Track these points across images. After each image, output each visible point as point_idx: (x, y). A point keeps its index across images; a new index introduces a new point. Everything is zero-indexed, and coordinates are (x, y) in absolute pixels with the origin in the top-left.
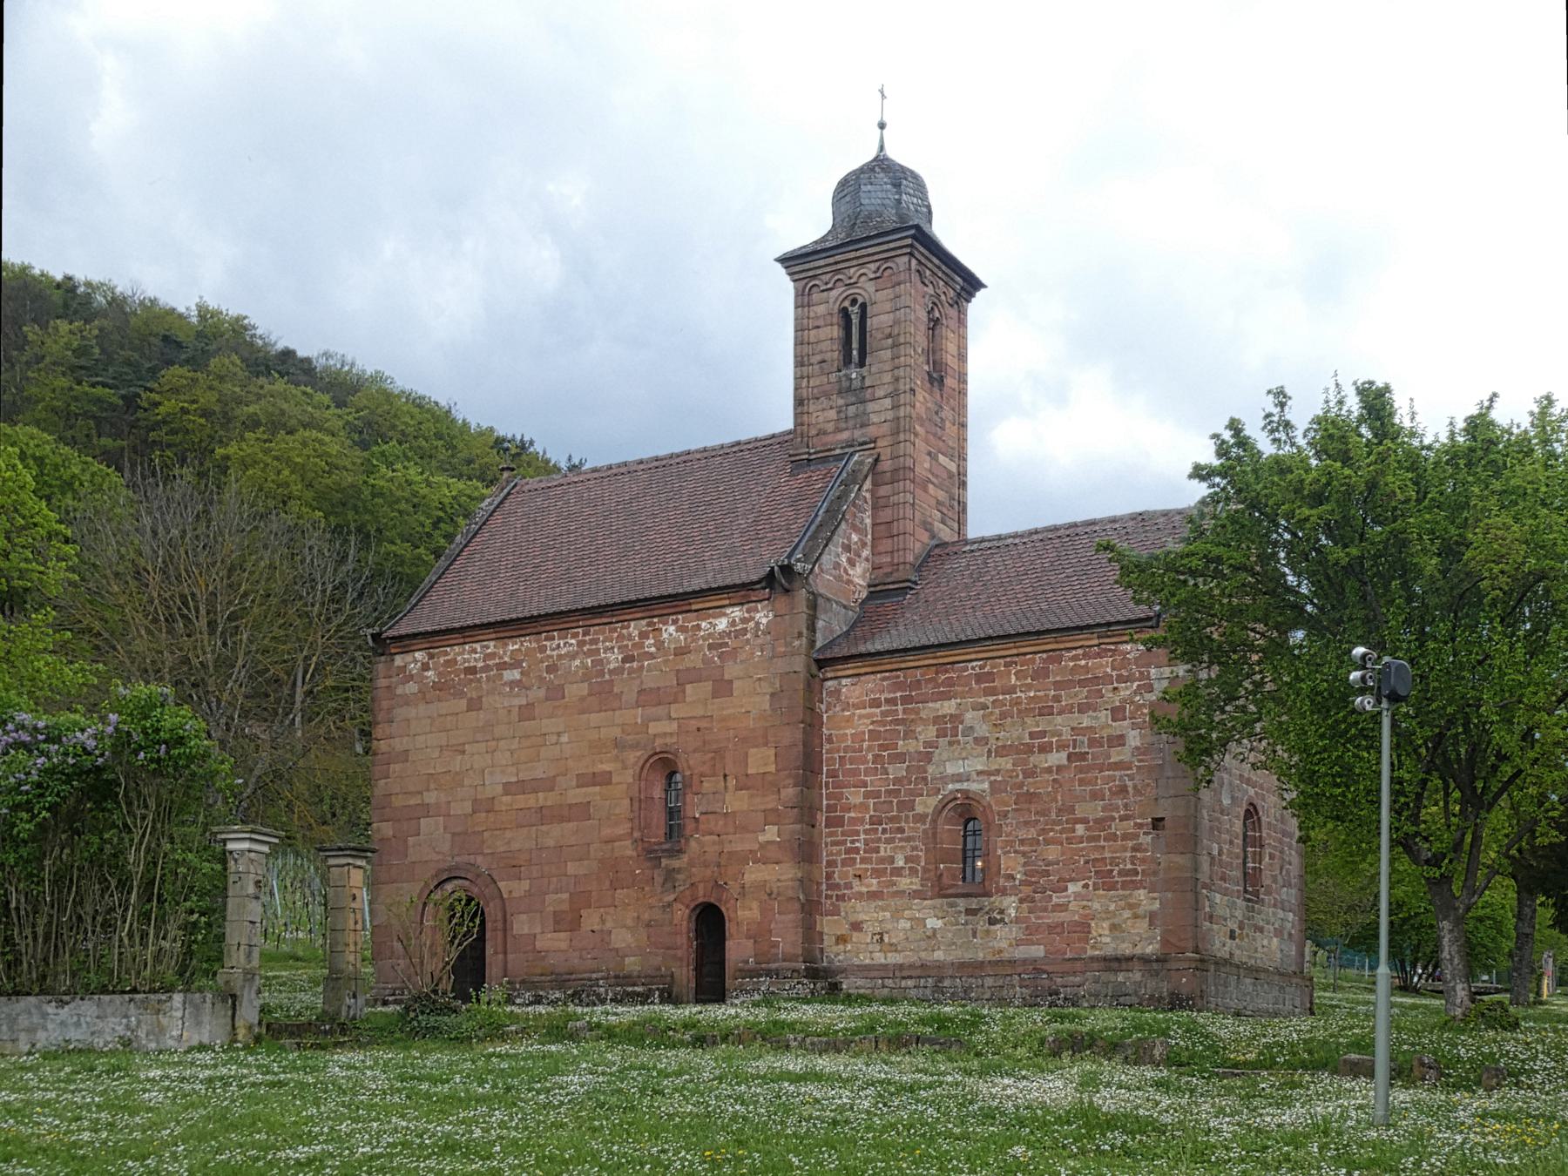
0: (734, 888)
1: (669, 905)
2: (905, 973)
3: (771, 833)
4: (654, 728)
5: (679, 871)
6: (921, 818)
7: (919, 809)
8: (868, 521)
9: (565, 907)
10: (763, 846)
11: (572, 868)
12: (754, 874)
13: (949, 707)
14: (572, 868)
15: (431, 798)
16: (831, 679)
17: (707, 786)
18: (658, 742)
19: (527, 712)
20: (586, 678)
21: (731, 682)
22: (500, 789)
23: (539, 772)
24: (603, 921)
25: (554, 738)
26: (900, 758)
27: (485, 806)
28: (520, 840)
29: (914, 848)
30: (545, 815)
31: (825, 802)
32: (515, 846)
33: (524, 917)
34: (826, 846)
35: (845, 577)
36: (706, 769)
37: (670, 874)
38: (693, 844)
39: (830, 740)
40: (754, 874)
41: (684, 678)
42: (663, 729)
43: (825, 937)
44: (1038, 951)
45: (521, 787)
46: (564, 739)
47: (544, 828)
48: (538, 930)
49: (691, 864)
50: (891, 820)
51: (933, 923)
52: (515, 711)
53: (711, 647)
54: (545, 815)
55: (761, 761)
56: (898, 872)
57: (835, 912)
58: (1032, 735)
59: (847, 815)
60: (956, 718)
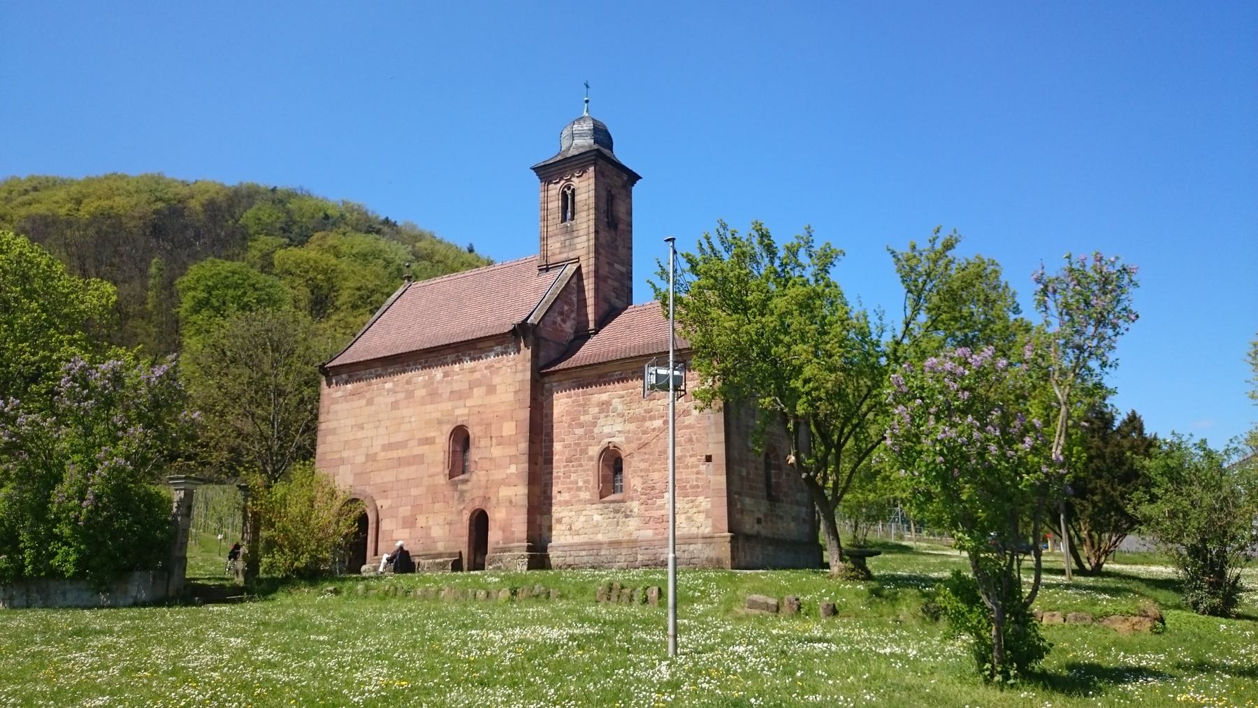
0: (494, 500)
2: (582, 548)
3: (513, 469)
4: (458, 412)
6: (591, 459)
7: (590, 453)
10: (508, 476)
11: (414, 492)
12: (505, 492)
13: (604, 397)
15: (345, 454)
17: (483, 443)
18: (460, 419)
19: (395, 406)
21: (495, 386)
23: (399, 437)
24: (427, 522)
26: (581, 425)
27: (371, 458)
28: (388, 477)
29: (588, 475)
30: (400, 462)
32: (386, 480)
37: (462, 493)
38: (474, 477)
40: (505, 492)
42: (461, 414)
44: (648, 533)
45: (389, 447)
46: (413, 419)
47: (400, 470)
48: (394, 527)
49: (472, 489)
50: (576, 459)
51: (597, 518)
53: (486, 368)
54: (400, 462)
56: (579, 489)
58: (646, 411)
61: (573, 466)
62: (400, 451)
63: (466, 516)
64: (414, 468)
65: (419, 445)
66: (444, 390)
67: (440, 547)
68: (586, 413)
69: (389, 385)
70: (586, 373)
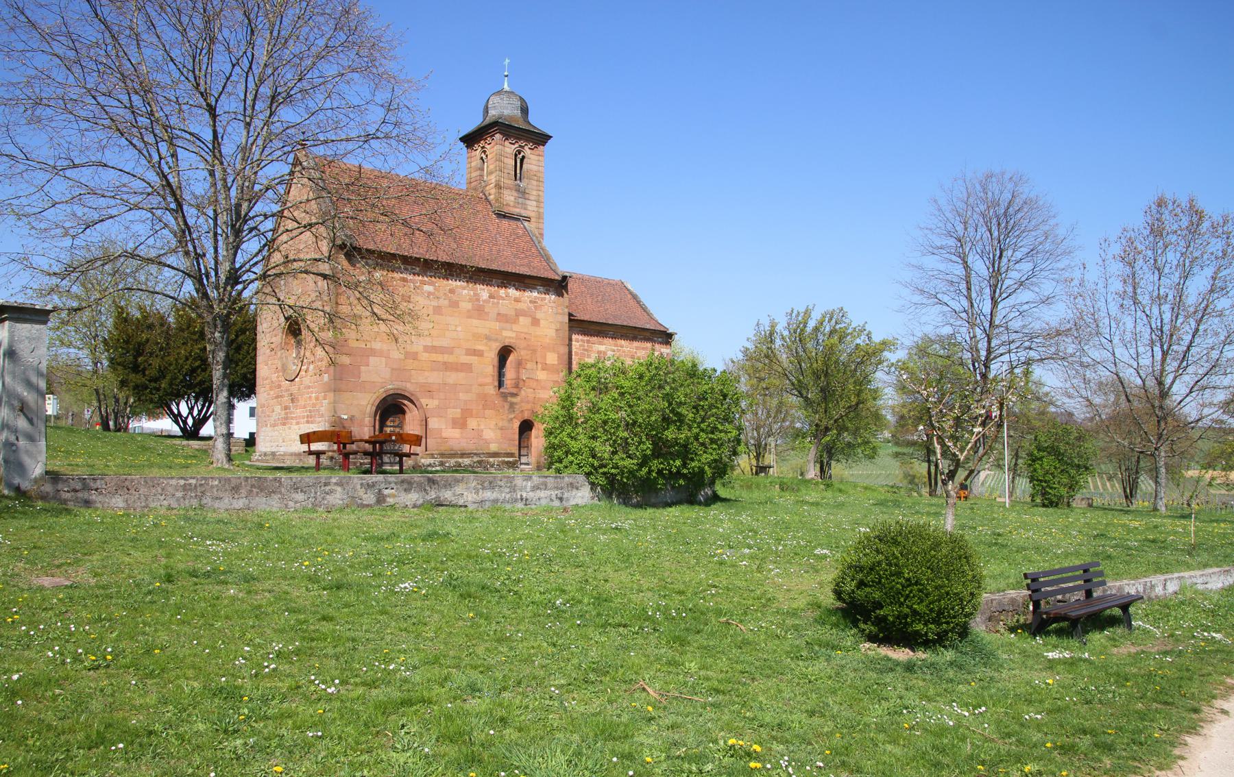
1: (511, 419)
4: (505, 333)
5: (516, 404)
9: (459, 416)
11: (462, 396)
13: (602, 348)
14: (462, 396)
17: (529, 366)
20: (470, 300)
22: (421, 348)
23: (444, 343)
24: (479, 425)
25: (453, 328)
28: (434, 378)
30: (448, 367)
32: (430, 381)
33: (435, 419)
36: (528, 357)
37: (512, 405)
38: (523, 392)
41: (519, 313)
42: (509, 336)
46: (459, 329)
47: (448, 373)
48: (444, 427)
49: (522, 401)
52: (431, 308)
53: (531, 302)
54: (448, 367)
55: (552, 359)
62: (446, 356)
63: (517, 424)
64: (462, 375)
65: (466, 355)
66: (491, 310)
67: (494, 448)
68: (589, 356)
69: (428, 288)
70: (593, 327)
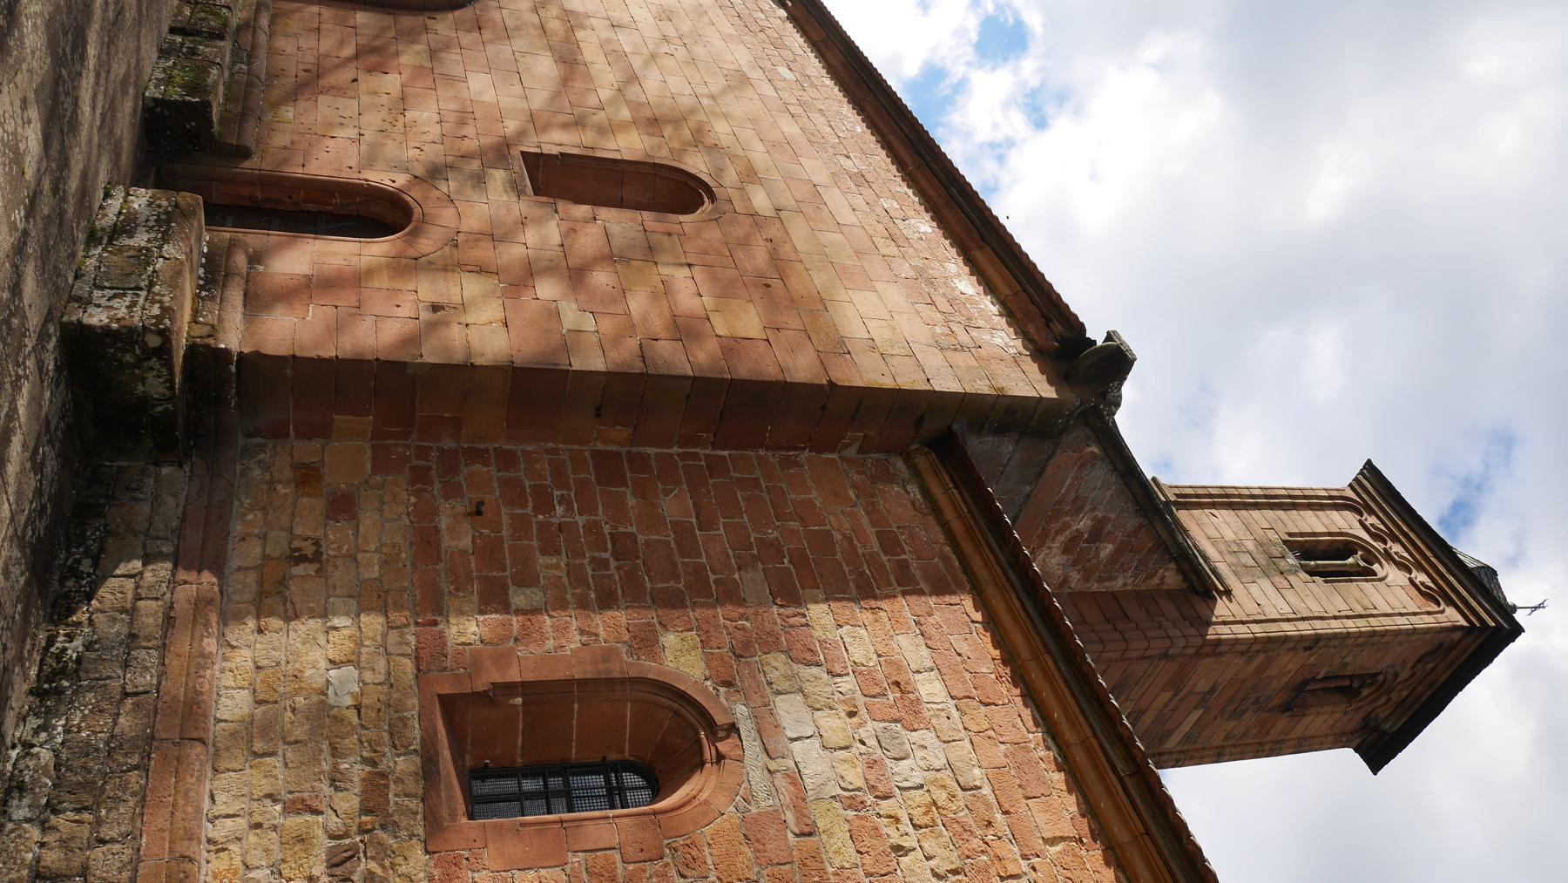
8: (1118, 584)
16: (912, 466)
31: (651, 451)
34: (549, 451)
35: (1055, 526)
39: (787, 463)
43: (316, 444)
57: (381, 463)
59: (628, 491)
60: (911, 713)
61: (601, 564)
